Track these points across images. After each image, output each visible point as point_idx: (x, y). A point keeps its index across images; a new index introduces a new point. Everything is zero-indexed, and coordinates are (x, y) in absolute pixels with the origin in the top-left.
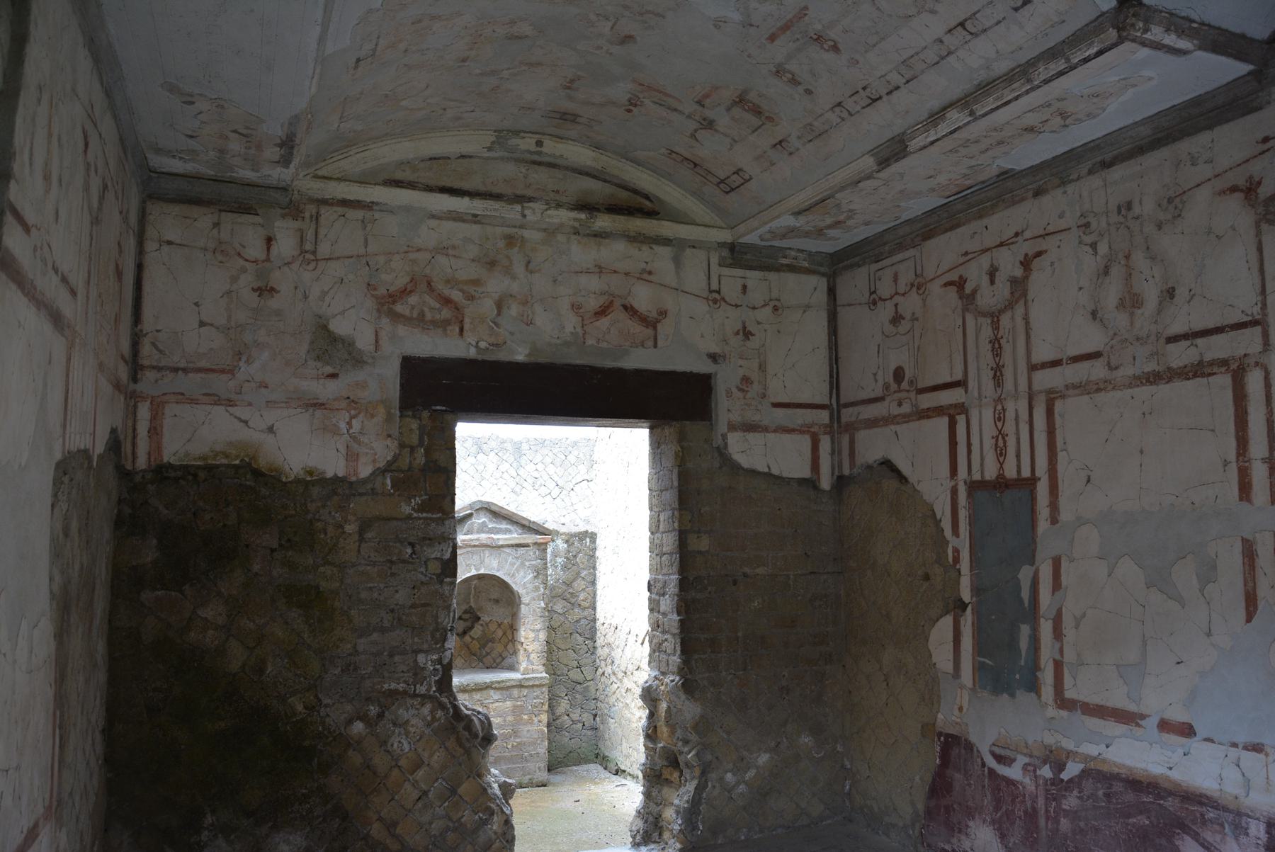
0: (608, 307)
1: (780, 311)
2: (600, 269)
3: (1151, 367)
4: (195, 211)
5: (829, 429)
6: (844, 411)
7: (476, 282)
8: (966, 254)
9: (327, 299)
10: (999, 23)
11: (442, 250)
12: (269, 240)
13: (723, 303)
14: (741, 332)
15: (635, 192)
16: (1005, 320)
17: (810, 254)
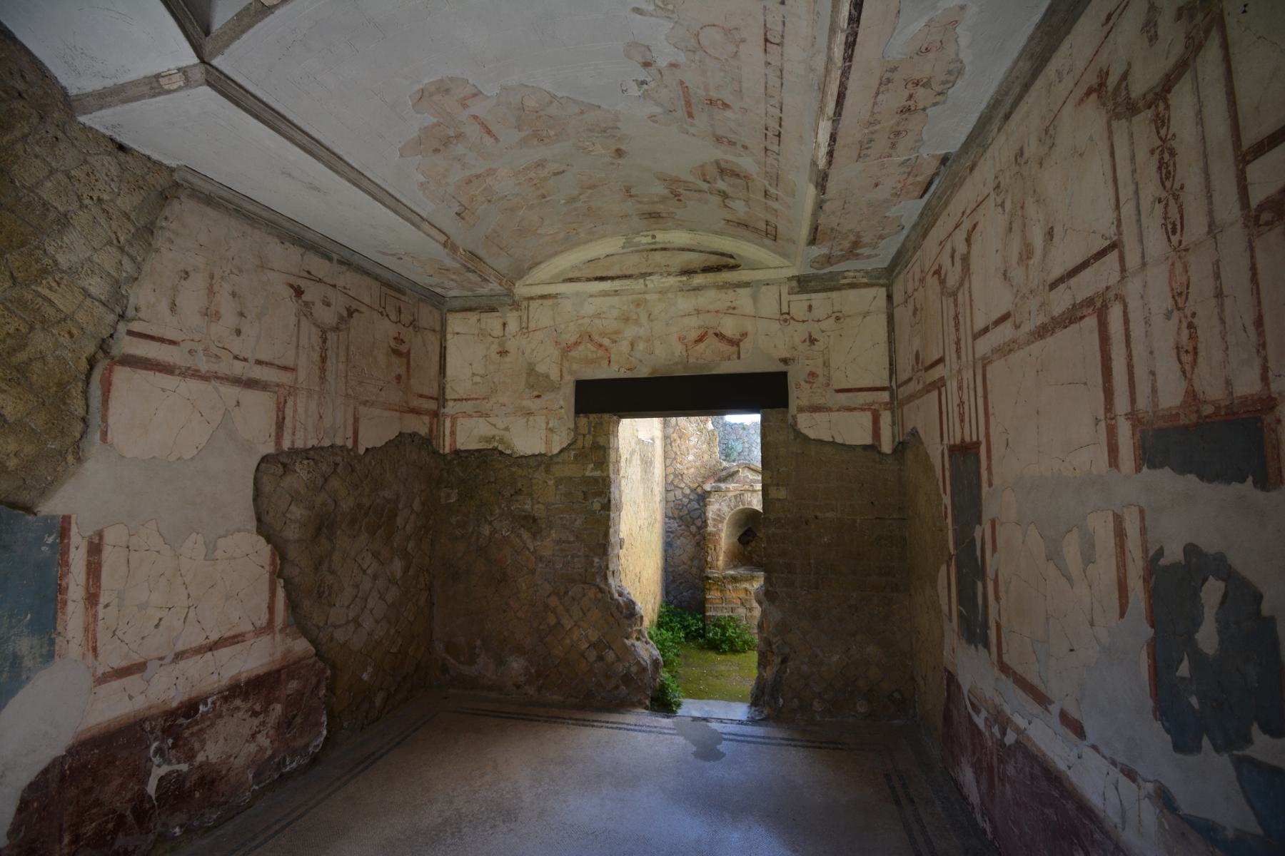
0: (704, 336)
1: (842, 320)
2: (698, 311)
3: (1041, 319)
4: (469, 314)
5: (890, 406)
6: (902, 389)
7: (616, 333)
8: (941, 243)
9: (535, 353)
10: (784, 23)
11: (598, 315)
12: (504, 325)
13: (792, 321)
14: (808, 340)
15: (723, 254)
16: (960, 295)
17: (867, 272)
